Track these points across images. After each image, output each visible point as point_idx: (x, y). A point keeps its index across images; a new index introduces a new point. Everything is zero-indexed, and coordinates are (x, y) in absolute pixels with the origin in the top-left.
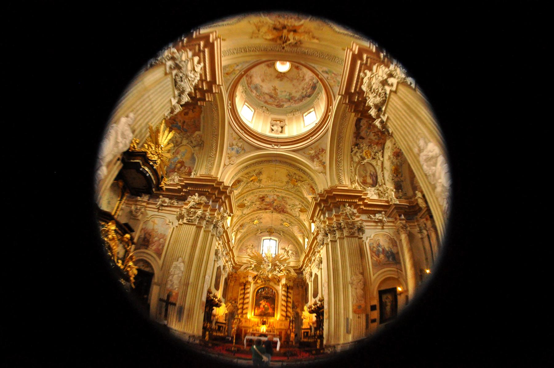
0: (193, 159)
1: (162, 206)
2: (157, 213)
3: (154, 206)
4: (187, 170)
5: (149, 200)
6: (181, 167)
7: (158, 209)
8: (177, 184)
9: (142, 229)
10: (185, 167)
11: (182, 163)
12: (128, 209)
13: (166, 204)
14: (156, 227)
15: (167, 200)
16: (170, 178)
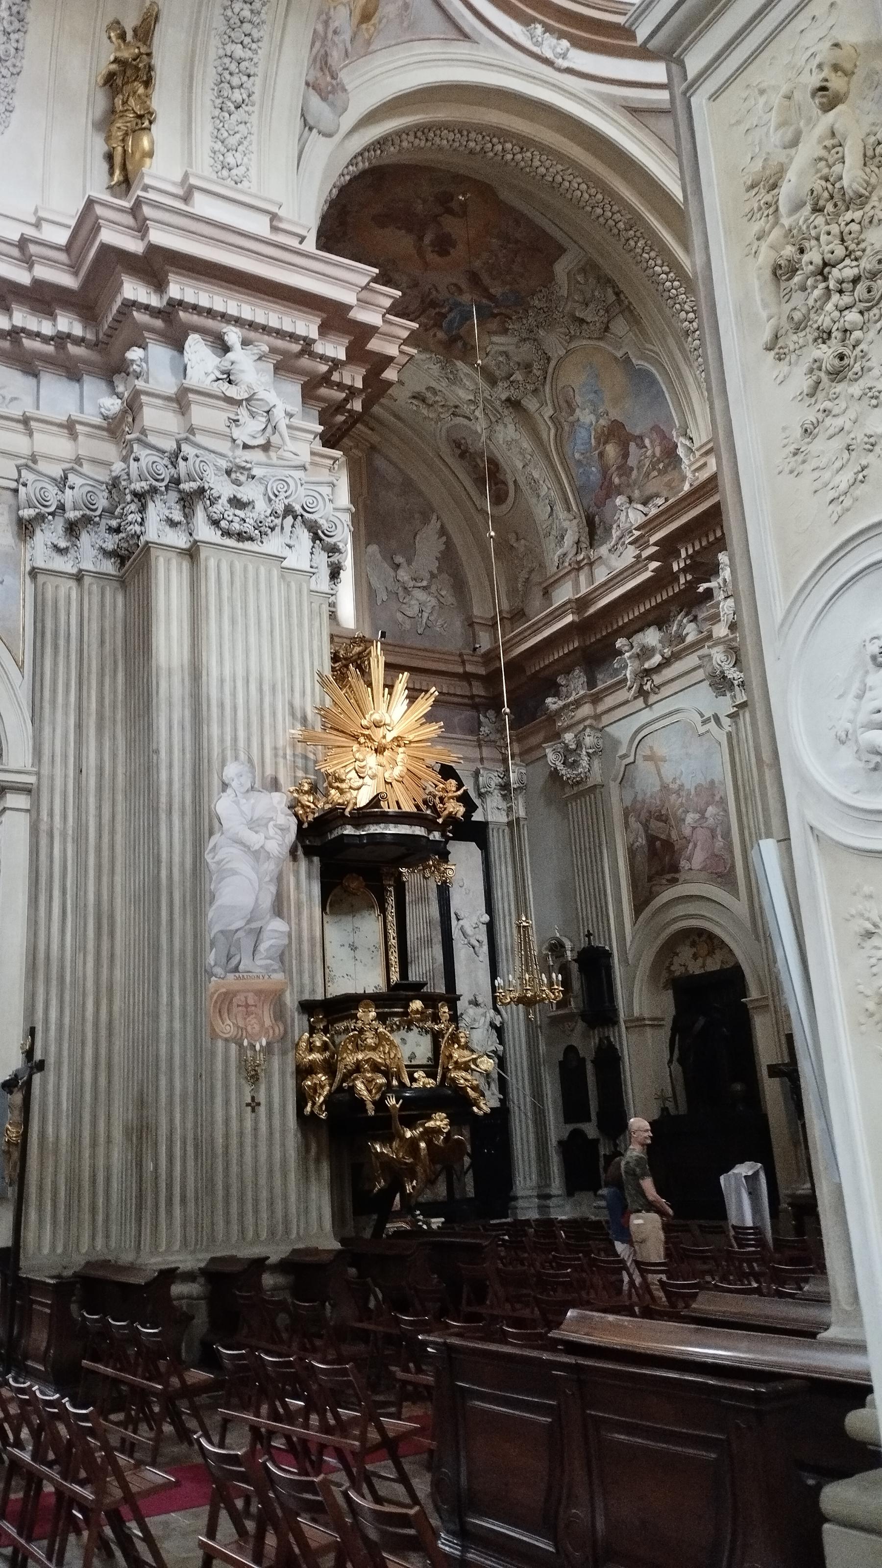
0: (642, 382)
1: (648, 672)
2: (646, 716)
3: (623, 695)
4: (653, 448)
5: (591, 683)
6: (626, 455)
7: (642, 693)
8: (639, 563)
9: (626, 813)
10: (639, 440)
11: (616, 432)
12: (540, 780)
13: (657, 659)
14: (668, 771)
15: (651, 637)
16: (615, 534)
